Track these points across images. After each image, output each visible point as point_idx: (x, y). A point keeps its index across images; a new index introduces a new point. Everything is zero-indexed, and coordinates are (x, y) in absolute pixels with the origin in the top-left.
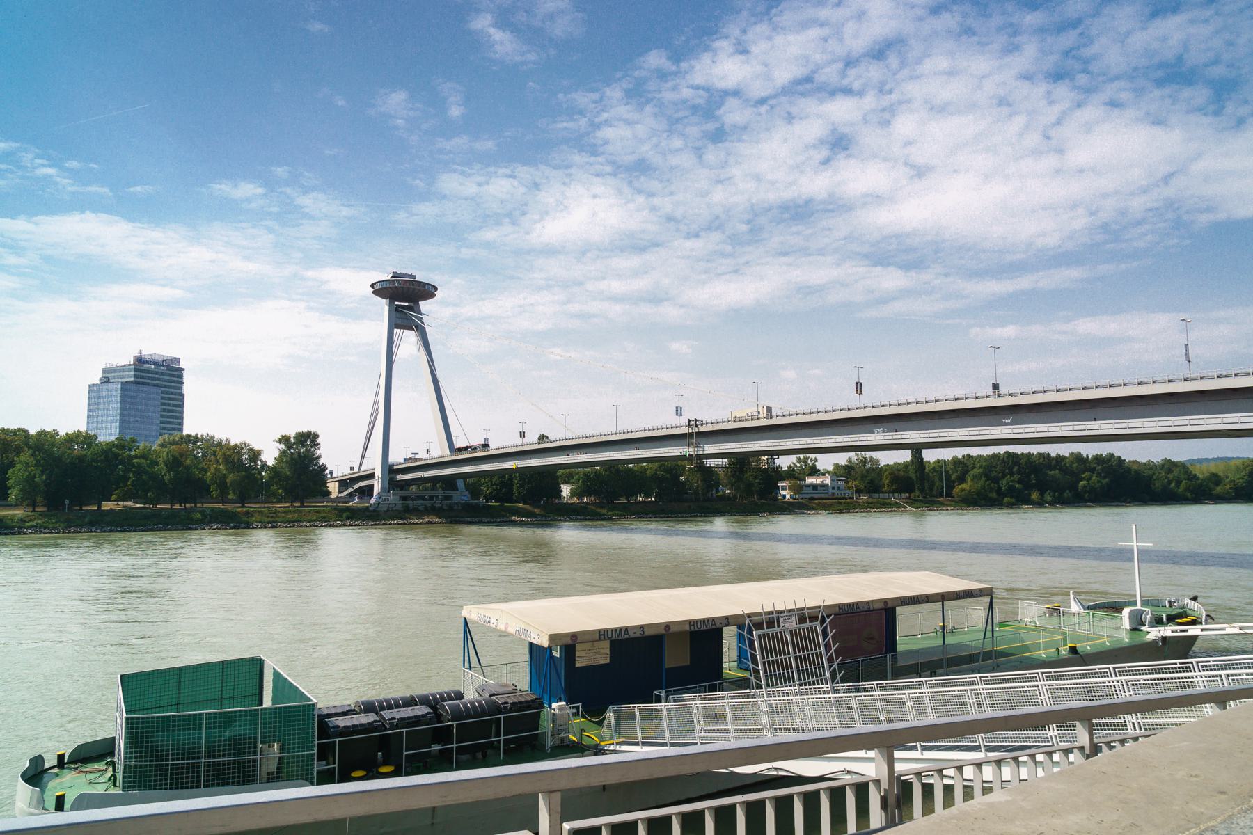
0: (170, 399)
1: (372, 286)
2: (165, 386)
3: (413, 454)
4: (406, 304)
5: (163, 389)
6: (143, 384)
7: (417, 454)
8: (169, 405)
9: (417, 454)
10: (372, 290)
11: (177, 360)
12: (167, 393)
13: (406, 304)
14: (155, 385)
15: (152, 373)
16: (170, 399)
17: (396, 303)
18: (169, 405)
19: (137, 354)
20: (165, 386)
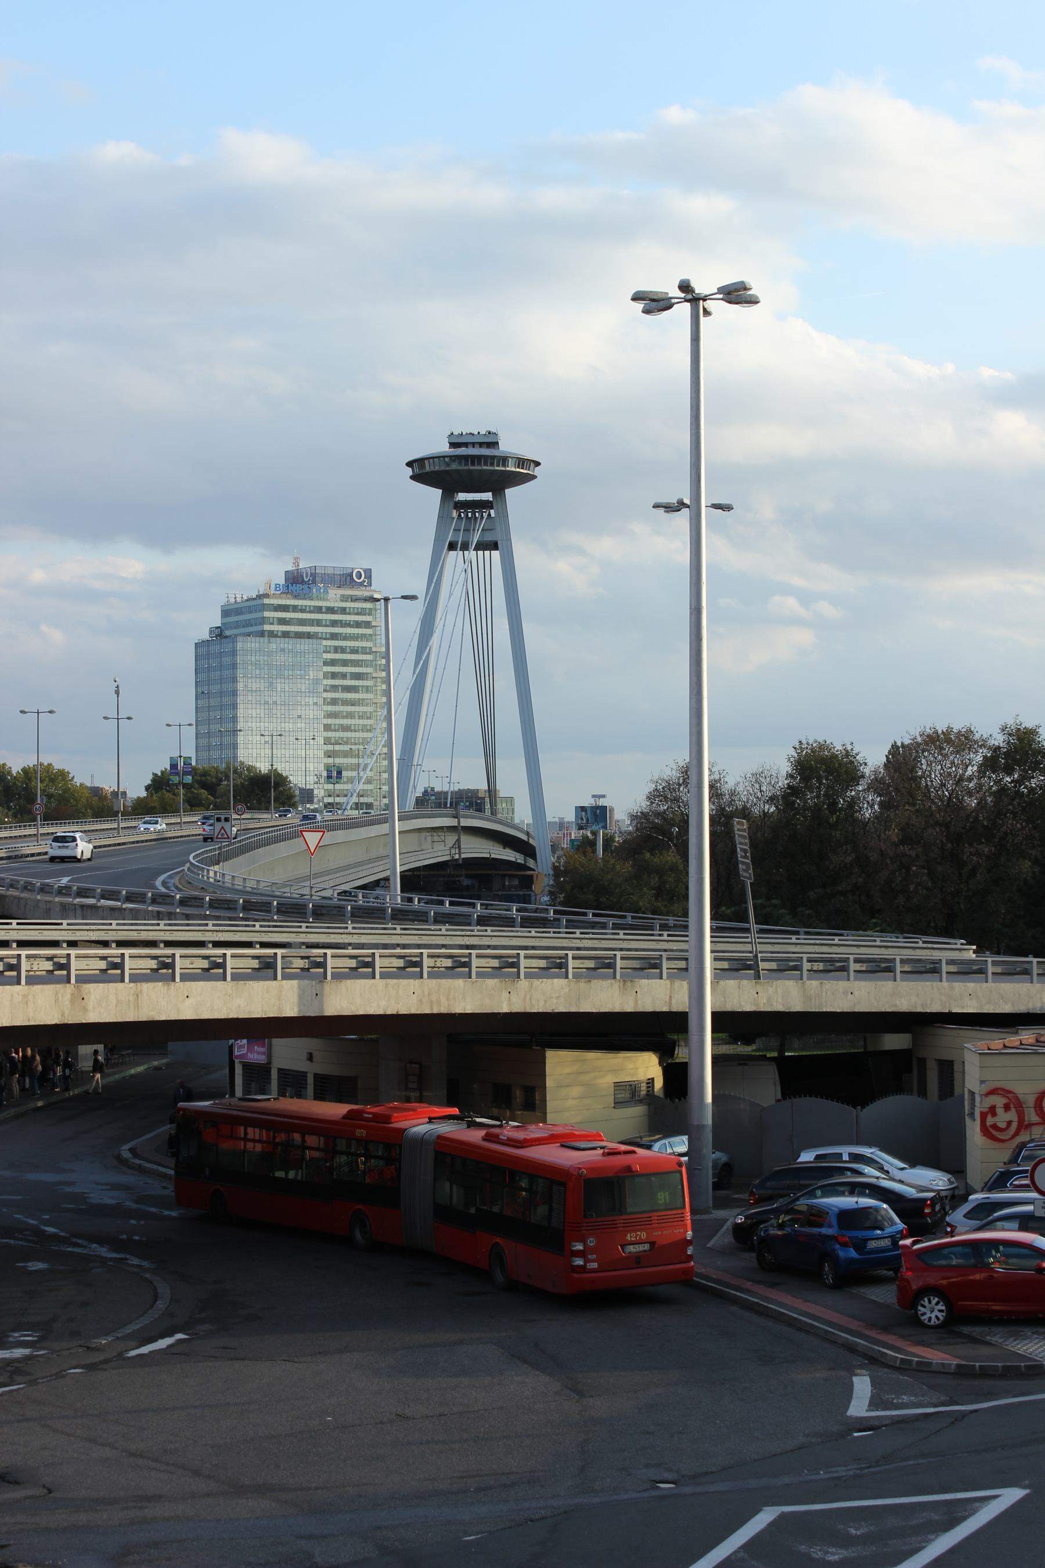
0: (345, 663)
1: (410, 464)
2: (334, 637)
3: (594, 796)
4: (487, 496)
5: (325, 643)
6: (286, 635)
7: (603, 796)
8: (344, 676)
9: (603, 796)
10: (409, 471)
11: (368, 573)
12: (336, 650)
13: (487, 496)
14: (309, 636)
15: (310, 612)
16: (345, 663)
17: (462, 496)
18: (344, 676)
19: (290, 567)
20: (334, 637)
